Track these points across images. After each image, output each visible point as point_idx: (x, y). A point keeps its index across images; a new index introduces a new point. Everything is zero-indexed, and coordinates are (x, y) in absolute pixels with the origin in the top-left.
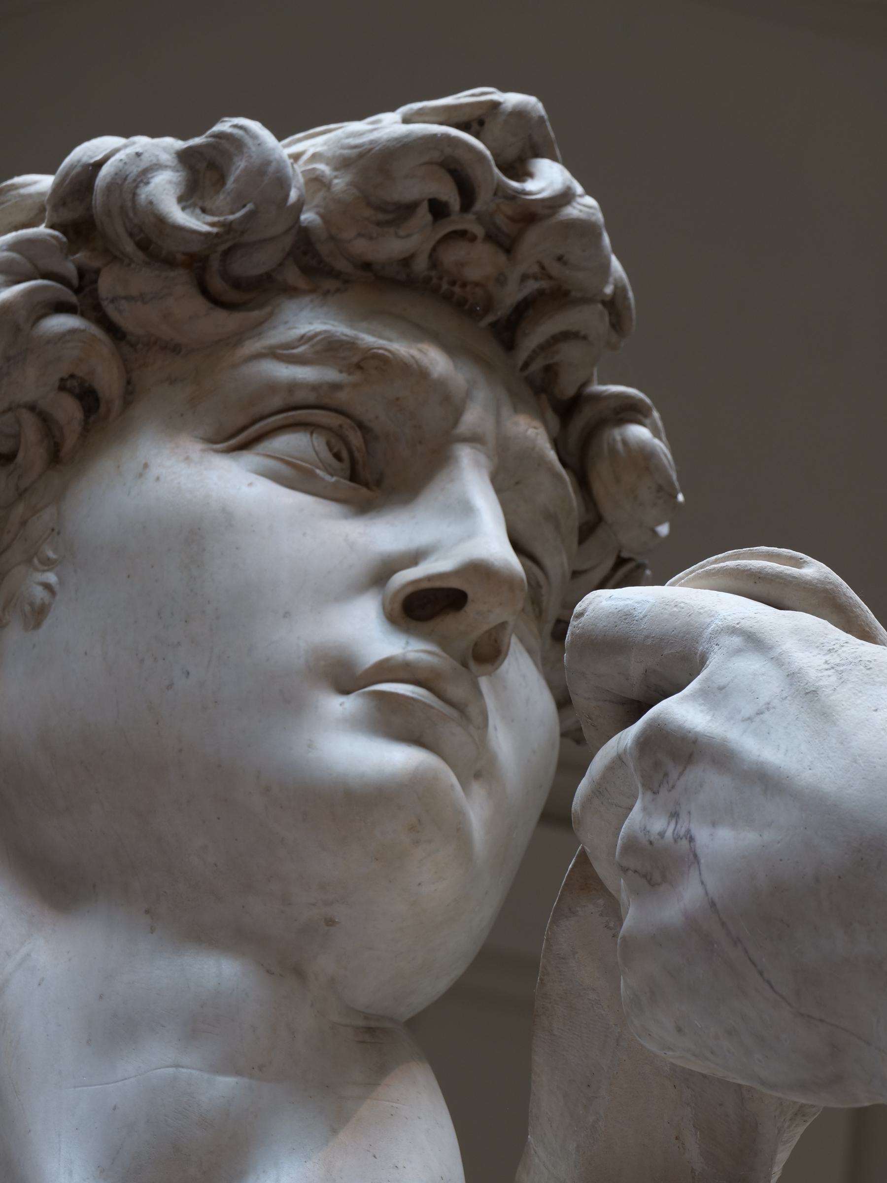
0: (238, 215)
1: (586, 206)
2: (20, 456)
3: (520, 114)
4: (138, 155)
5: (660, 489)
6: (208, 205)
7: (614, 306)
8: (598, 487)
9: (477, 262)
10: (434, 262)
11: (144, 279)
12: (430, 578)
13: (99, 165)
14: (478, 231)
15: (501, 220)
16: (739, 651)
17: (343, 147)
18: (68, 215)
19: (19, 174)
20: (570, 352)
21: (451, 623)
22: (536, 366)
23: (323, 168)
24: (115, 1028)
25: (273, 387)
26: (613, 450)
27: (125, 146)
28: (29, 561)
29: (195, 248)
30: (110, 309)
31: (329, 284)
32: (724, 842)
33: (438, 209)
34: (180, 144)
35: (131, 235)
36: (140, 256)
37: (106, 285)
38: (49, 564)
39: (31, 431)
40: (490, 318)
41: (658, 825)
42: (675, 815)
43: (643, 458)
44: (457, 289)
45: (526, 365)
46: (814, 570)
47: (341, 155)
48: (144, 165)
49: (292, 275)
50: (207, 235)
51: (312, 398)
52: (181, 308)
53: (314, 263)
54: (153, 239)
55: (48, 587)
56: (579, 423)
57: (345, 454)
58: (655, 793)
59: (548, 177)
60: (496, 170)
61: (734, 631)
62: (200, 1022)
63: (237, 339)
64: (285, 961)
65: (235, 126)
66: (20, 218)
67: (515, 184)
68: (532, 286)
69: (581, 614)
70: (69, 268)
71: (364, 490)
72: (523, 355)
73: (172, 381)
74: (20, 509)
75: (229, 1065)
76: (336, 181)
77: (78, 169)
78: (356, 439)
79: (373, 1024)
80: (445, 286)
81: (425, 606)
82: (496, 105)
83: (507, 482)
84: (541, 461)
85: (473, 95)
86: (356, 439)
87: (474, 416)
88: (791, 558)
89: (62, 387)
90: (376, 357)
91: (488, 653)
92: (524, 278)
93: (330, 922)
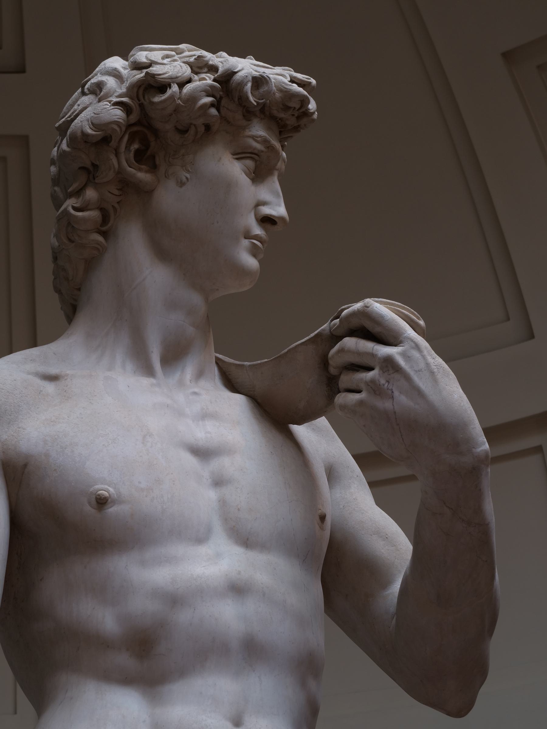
2: (186, 135)
12: (271, 215)
14: (296, 115)
16: (413, 348)
17: (281, 85)
37: (223, 102)
38: (188, 171)
41: (383, 381)
42: (388, 382)
46: (422, 323)
54: (242, 100)
55: (187, 178)
63: (244, 128)
66: (200, 65)
82: (310, 83)
90: (273, 147)
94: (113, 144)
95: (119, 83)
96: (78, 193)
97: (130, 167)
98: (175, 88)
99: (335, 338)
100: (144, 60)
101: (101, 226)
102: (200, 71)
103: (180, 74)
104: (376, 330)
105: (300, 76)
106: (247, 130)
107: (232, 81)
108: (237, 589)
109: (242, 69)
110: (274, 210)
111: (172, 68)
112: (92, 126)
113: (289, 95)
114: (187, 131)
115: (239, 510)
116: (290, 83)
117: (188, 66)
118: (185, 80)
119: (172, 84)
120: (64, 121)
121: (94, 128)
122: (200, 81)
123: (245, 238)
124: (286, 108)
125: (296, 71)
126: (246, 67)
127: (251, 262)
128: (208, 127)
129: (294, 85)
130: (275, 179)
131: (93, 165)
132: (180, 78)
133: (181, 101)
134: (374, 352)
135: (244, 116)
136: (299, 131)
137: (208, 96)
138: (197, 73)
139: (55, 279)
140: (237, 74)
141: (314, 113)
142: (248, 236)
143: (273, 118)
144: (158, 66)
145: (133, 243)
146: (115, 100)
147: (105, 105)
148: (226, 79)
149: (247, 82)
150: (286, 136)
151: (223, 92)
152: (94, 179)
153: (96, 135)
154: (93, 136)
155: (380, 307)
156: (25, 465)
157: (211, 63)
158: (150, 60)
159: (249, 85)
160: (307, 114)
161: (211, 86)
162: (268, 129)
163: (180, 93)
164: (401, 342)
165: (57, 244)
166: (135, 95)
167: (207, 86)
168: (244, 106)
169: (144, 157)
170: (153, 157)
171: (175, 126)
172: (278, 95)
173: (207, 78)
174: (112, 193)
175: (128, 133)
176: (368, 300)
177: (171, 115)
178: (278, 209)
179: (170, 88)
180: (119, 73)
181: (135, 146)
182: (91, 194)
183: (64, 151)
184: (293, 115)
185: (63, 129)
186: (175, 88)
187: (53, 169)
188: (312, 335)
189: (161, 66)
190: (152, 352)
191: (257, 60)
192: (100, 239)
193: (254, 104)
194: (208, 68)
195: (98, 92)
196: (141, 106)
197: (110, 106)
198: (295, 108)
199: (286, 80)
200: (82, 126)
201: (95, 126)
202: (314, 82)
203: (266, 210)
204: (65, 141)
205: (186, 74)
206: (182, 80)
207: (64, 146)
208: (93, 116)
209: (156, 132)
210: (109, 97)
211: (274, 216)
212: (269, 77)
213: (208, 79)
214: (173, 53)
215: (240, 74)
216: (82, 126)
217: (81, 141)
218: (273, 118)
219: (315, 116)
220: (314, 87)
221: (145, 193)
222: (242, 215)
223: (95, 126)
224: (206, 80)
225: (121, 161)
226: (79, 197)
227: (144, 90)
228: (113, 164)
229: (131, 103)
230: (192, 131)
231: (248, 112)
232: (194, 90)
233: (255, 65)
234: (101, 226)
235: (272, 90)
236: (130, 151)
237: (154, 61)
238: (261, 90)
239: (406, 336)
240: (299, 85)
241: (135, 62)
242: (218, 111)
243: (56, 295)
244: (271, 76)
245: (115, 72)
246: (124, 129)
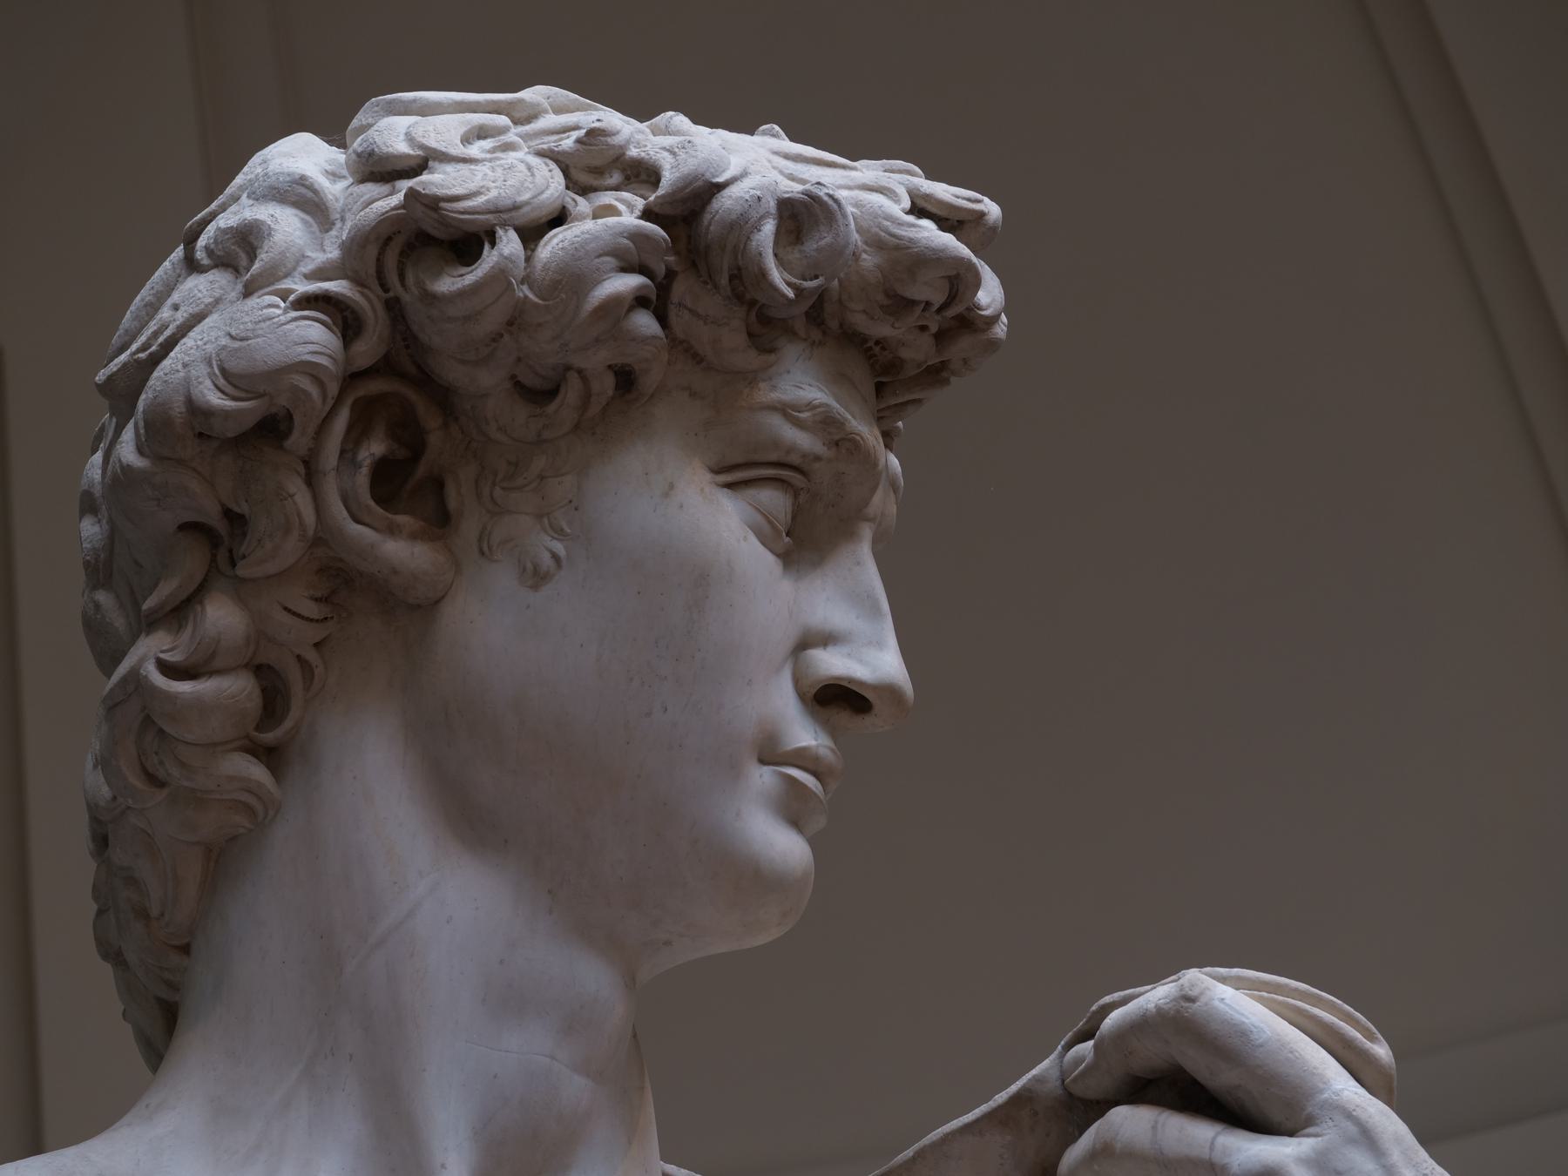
2: (551, 408)
12: (851, 680)
13: (720, 187)
14: (934, 328)
16: (1352, 1141)
17: (879, 226)
25: (776, 444)
28: (539, 517)
37: (679, 289)
38: (559, 533)
44: (877, 349)
46: (1382, 1051)
47: (876, 234)
49: (800, 325)
52: (732, 340)
54: (744, 284)
55: (555, 557)
61: (1349, 1115)
63: (750, 379)
65: (831, 196)
66: (597, 162)
73: (693, 395)
76: (864, 256)
77: (700, 183)
80: (871, 344)
82: (981, 215)
85: (969, 200)
88: (1368, 1029)
94: (298, 441)
95: (315, 228)
96: (178, 613)
97: (358, 521)
98: (510, 244)
99: (1080, 1108)
100: (402, 147)
101: (258, 728)
102: (595, 183)
103: (526, 196)
104: (1218, 1078)
105: (944, 191)
106: (762, 385)
107: (707, 217)
109: (744, 174)
110: (861, 661)
111: (499, 170)
112: (221, 382)
114: (551, 393)
116: (911, 219)
117: (553, 166)
118: (544, 214)
119: (500, 232)
120: (125, 365)
121: (229, 389)
122: (595, 217)
123: (763, 761)
124: (899, 305)
125: (930, 176)
126: (756, 164)
127: (783, 846)
128: (626, 379)
129: (927, 223)
130: (865, 550)
131: (228, 513)
133: (531, 288)
134: (1217, 1157)
135: (750, 335)
136: (946, 382)
137: (626, 269)
138: (585, 191)
139: (100, 913)
140: (726, 192)
141: (994, 319)
142: (770, 753)
143: (851, 339)
144: (449, 168)
145: (369, 783)
146: (302, 287)
147: (267, 305)
148: (688, 210)
149: (762, 218)
150: (900, 400)
151: (677, 253)
152: (233, 564)
153: (239, 411)
154: (226, 414)
155: (1236, 1000)
157: (633, 152)
158: (422, 147)
159: (769, 227)
160: (970, 323)
161: (636, 236)
162: (838, 379)
163: (528, 259)
164: (1310, 1121)
165: (105, 791)
166: (372, 270)
167: (621, 234)
168: (752, 303)
169: (404, 485)
171: (513, 377)
172: (869, 260)
173: (621, 207)
174: (294, 614)
175: (349, 401)
176: (1194, 977)
177: (497, 338)
178: (877, 660)
179: (493, 244)
180: (315, 192)
181: (376, 447)
182: (221, 617)
183: (127, 469)
184: (923, 328)
185: (123, 392)
186: (510, 244)
187: (90, 530)
188: (1001, 1098)
189: (460, 166)
190: (443, 1166)
191: (794, 138)
192: (257, 772)
193: (784, 295)
194: (623, 170)
195: (244, 261)
196: (394, 308)
197: (286, 311)
198: (928, 304)
199: (897, 209)
200: (187, 381)
201: (232, 379)
202: (992, 209)
203: (834, 663)
204: (128, 434)
205: (544, 196)
207: (127, 451)
208: (224, 348)
209: (444, 398)
210: (279, 279)
211: (861, 683)
212: (836, 201)
213: (626, 212)
214: (503, 120)
215: (734, 191)
216: (187, 381)
217: (185, 434)
218: (851, 339)
219: (1001, 330)
220: (993, 229)
221: (409, 611)
222: (750, 682)
223: (232, 379)
224: (619, 214)
225: (328, 500)
226: (180, 628)
227: (402, 254)
228: (299, 515)
229: (357, 297)
230: (571, 393)
231: (765, 320)
232: (577, 252)
233: (787, 157)
234: (258, 728)
235: (847, 244)
236: (356, 465)
237: (435, 150)
238: (811, 246)
239: (1326, 1101)
240: (944, 224)
241: (371, 154)
242: (662, 319)
243: (107, 969)
244: (842, 194)
245: (303, 190)
246: (333, 389)
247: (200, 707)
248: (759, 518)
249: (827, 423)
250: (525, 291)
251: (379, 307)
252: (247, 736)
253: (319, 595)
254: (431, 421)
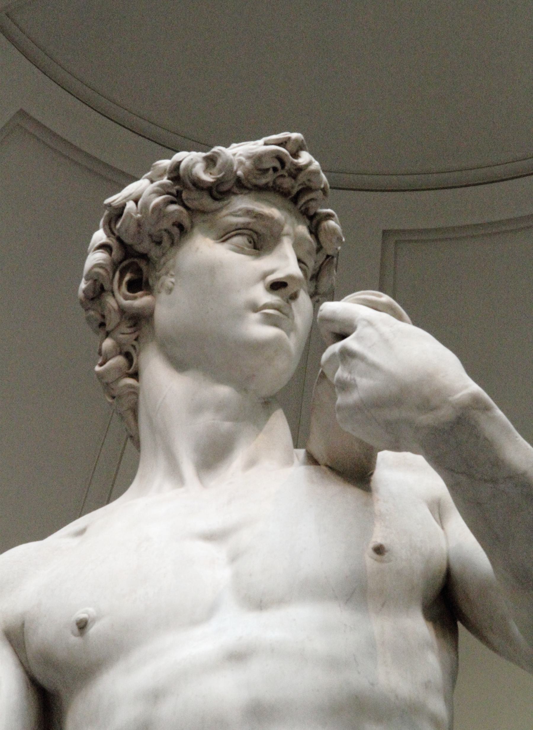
0: (221, 175)
1: (316, 165)
3: (296, 140)
4: (192, 159)
5: (338, 238)
6: (212, 172)
7: (324, 190)
8: (321, 239)
9: (287, 183)
10: (274, 182)
11: (195, 194)
12: (277, 279)
14: (286, 174)
15: (292, 170)
18: (173, 175)
19: (158, 160)
20: (312, 204)
21: (283, 291)
22: (303, 208)
23: (243, 159)
24: (197, 409)
26: (325, 230)
27: (188, 156)
29: (209, 185)
30: (186, 202)
31: (247, 191)
32: (365, 384)
33: (275, 169)
34: (204, 154)
35: (191, 182)
36: (193, 188)
37: (184, 195)
38: (172, 276)
39: (166, 238)
40: (290, 197)
42: (350, 372)
43: (333, 231)
45: (300, 208)
46: (385, 298)
48: (193, 162)
49: (235, 190)
50: (212, 183)
51: (242, 226)
53: (242, 186)
54: (198, 185)
55: (172, 283)
56: (315, 222)
57: (252, 241)
58: (344, 365)
59: (305, 158)
60: (291, 157)
61: (364, 320)
62: (220, 407)
64: (242, 384)
66: (159, 174)
67: (295, 161)
68: (301, 187)
69: (321, 311)
70: (174, 191)
71: (257, 251)
72: (299, 206)
73: (204, 221)
74: (163, 260)
75: (228, 419)
78: (255, 237)
79: (266, 400)
80: (277, 189)
81: (276, 286)
82: (289, 138)
83: (297, 244)
84: (306, 239)
86: (255, 237)
87: (287, 228)
89: (174, 224)
90: (260, 214)
91: (294, 297)
92: (299, 185)
93: (254, 376)
94: (107, 286)
98: (130, 205)
104: (337, 329)
108: (237, 657)
113: (258, 159)
115: (251, 575)
124: (265, 171)
127: (269, 332)
132: (133, 194)
137: (161, 194)
142: (255, 308)
156: (23, 624)
160: (300, 169)
161: (162, 186)
167: (155, 187)
169: (138, 285)
170: (147, 282)
177: (139, 232)
181: (127, 278)
182: (108, 343)
186: (130, 205)
192: (130, 381)
196: (119, 239)
201: (87, 280)
206: (137, 195)
209: (144, 257)
211: (280, 279)
222: (239, 291)
225: (120, 298)
228: (111, 306)
230: (166, 238)
235: (227, 160)
246: (109, 269)
247: (108, 371)
248: (232, 247)
249: (248, 212)
250: (139, 215)
251: (114, 241)
252: (127, 374)
253: (129, 325)
254: (143, 265)
